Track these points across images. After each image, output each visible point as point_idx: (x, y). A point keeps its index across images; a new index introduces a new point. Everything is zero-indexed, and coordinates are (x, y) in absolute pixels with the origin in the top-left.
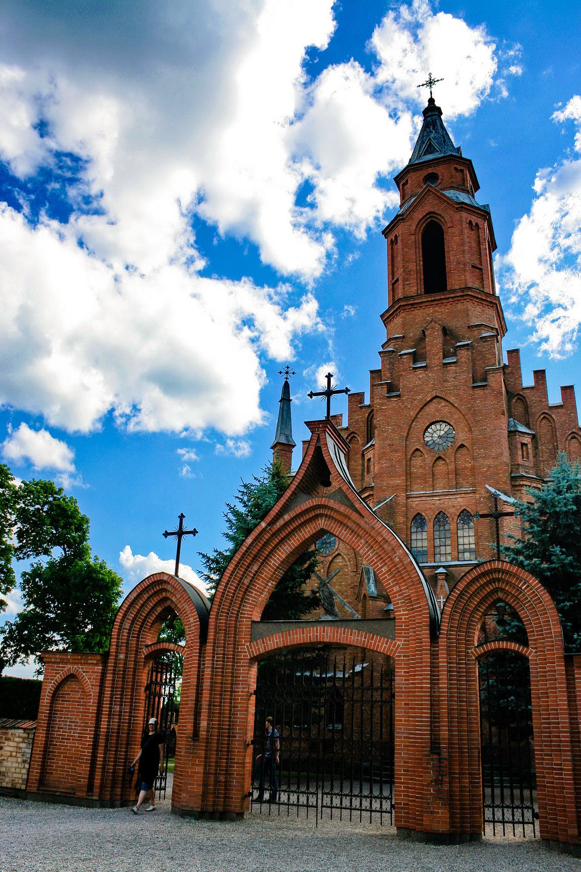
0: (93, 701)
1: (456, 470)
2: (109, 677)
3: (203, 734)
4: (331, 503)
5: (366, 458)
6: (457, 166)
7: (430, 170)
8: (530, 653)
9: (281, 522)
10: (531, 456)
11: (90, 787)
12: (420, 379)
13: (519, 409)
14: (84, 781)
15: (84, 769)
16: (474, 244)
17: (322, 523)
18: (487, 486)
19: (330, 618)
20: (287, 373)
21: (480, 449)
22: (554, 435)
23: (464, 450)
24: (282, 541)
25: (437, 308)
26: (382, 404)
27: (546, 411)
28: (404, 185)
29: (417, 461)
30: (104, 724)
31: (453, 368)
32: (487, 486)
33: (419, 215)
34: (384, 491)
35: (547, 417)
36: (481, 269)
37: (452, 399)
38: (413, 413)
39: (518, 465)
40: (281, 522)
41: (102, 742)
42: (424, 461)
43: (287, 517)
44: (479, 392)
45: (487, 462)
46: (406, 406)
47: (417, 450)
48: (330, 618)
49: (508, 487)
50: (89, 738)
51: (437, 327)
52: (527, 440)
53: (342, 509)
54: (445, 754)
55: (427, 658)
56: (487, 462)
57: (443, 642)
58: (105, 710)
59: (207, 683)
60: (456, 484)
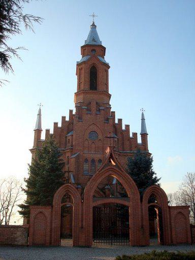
0: (49, 219)
3: (84, 226)
5: (68, 138)
7: (93, 48)
11: (50, 243)
14: (48, 241)
15: (48, 238)
30: (53, 226)
37: (98, 125)
40: (101, 172)
44: (106, 124)
53: (118, 170)
58: (53, 222)
59: (84, 214)
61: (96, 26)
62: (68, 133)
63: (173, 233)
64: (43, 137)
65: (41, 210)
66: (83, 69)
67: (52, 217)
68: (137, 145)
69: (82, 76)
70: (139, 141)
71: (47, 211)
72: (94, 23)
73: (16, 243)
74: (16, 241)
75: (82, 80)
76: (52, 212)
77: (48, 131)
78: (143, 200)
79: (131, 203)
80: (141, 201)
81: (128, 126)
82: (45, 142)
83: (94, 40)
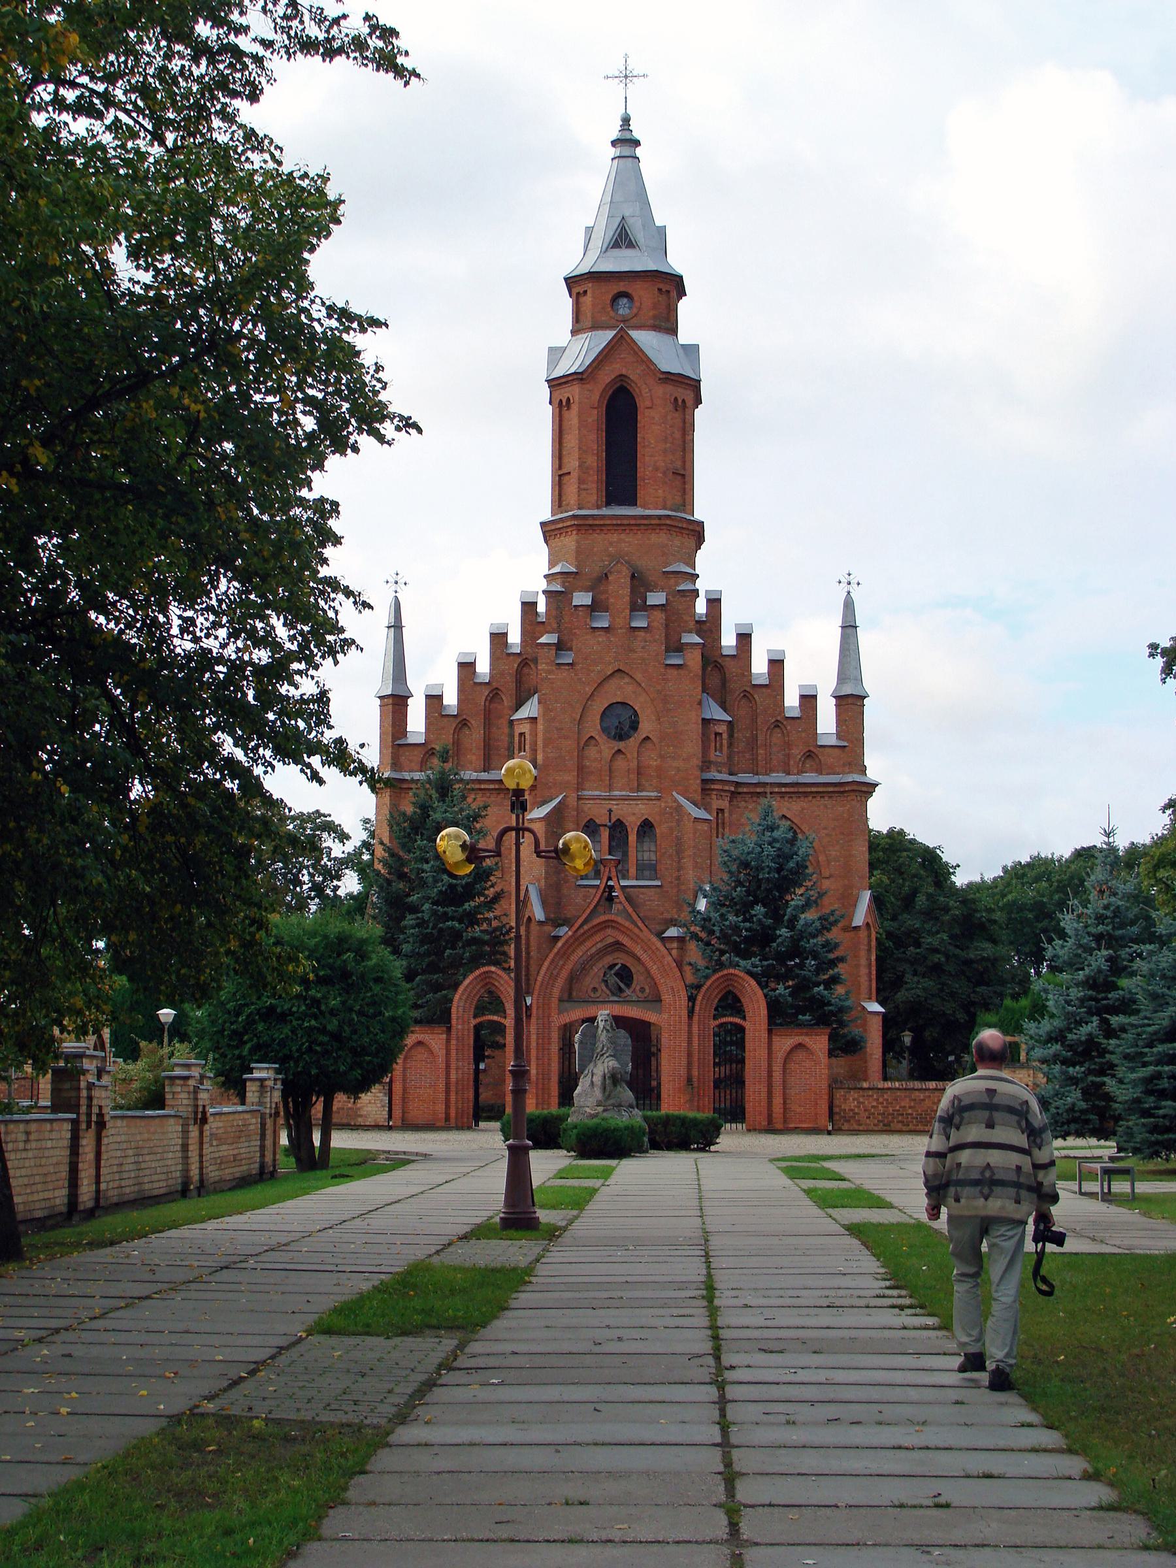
0: (441, 1060)
1: (639, 767)
2: (453, 1042)
4: (619, 919)
5: (518, 729)
6: (661, 286)
7: (621, 287)
8: (747, 1025)
9: (582, 931)
10: (725, 749)
11: (447, 1118)
12: (599, 643)
13: (714, 681)
15: (441, 1108)
16: (678, 435)
17: (609, 931)
18: (674, 793)
19: (616, 999)
20: (396, 583)
21: (668, 746)
22: (754, 719)
23: (648, 745)
24: (581, 943)
25: (623, 536)
26: (549, 672)
27: (748, 689)
28: (578, 294)
29: (592, 752)
30: (453, 1076)
31: (642, 634)
32: (674, 793)
33: (606, 376)
34: (550, 788)
35: (747, 695)
36: (683, 475)
37: (639, 676)
38: (589, 690)
39: (710, 762)
40: (582, 931)
41: (453, 1088)
42: (600, 752)
43: (586, 927)
45: (675, 764)
46: (580, 679)
47: (592, 737)
48: (616, 999)
49: (698, 797)
50: (442, 1085)
51: (626, 572)
52: (722, 729)
53: (627, 924)
54: (696, 1085)
55: (685, 1027)
56: (675, 764)
57: (696, 1018)
58: (453, 1066)
60: (639, 785)
61: (637, 143)
62: (519, 705)
63: (778, 1101)
64: (416, 721)
65: (420, 1037)
66: (575, 408)
67: (448, 1053)
68: (813, 754)
69: (572, 441)
70: (827, 721)
71: (435, 1040)
72: (626, 121)
73: (360, 1121)
74: (361, 1116)
75: (572, 464)
76: (448, 1040)
77: (434, 701)
78: (697, 1008)
79: (665, 1016)
80: (691, 1012)
81: (776, 665)
82: (427, 750)
83: (622, 239)
